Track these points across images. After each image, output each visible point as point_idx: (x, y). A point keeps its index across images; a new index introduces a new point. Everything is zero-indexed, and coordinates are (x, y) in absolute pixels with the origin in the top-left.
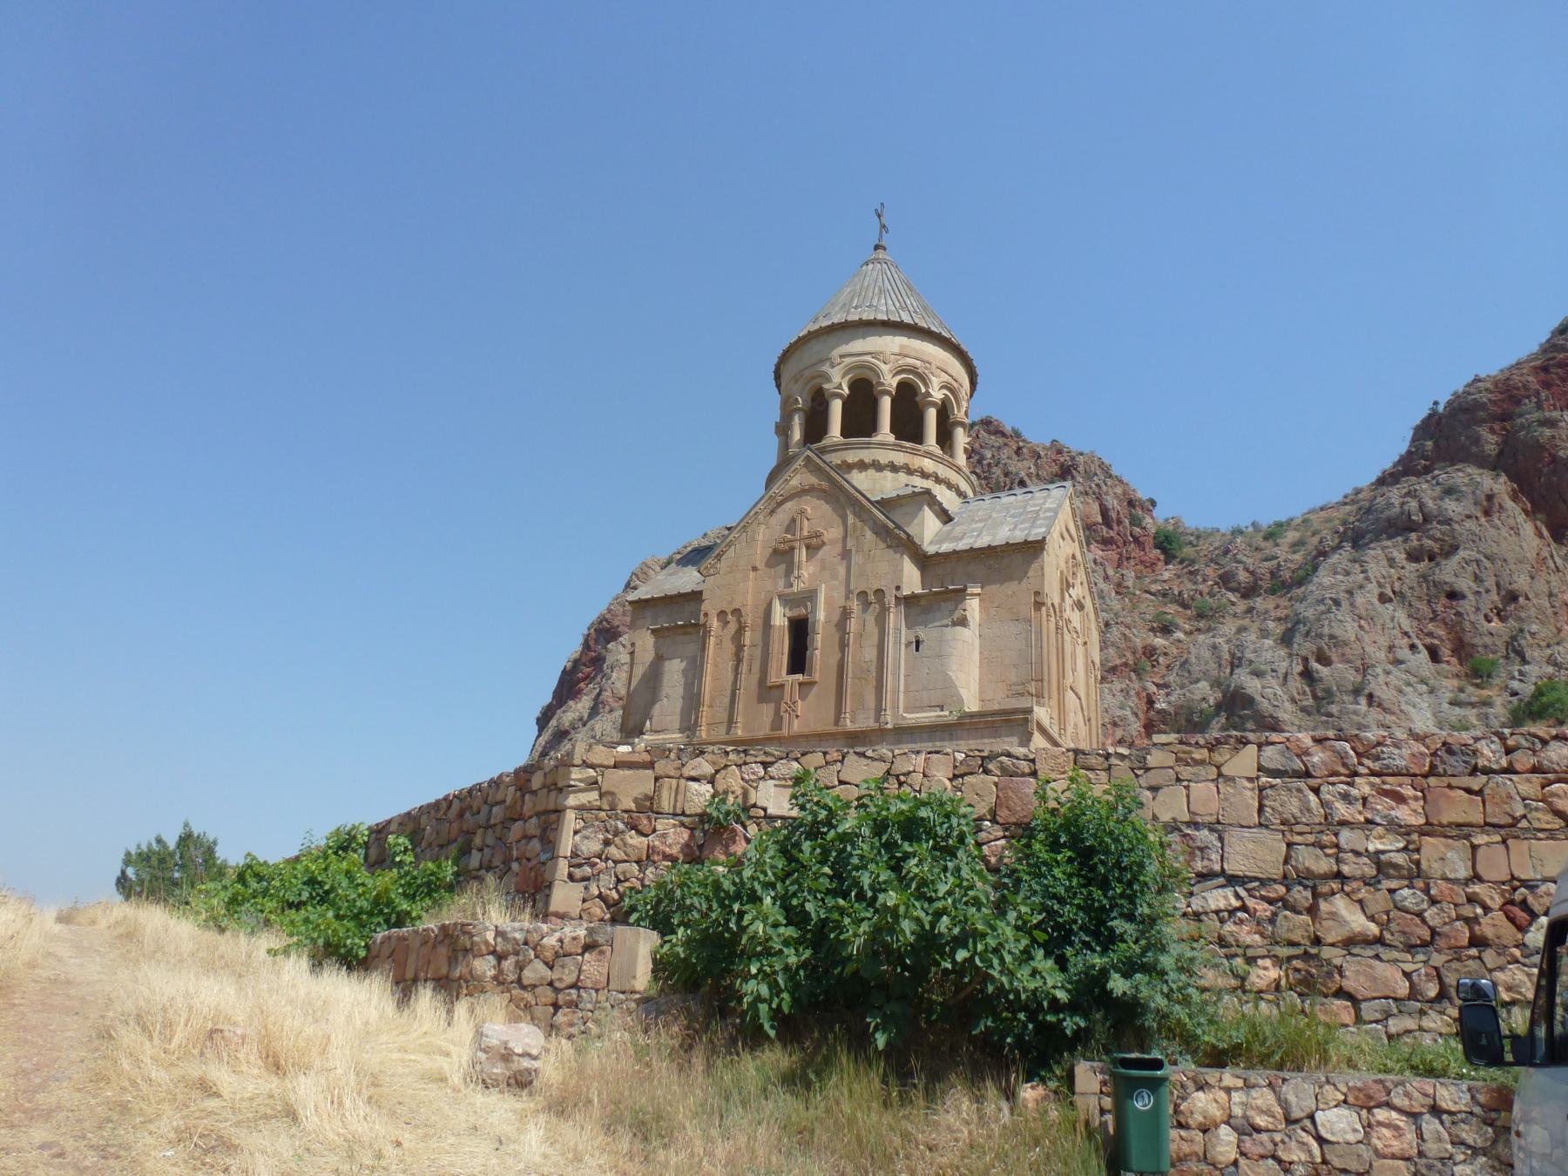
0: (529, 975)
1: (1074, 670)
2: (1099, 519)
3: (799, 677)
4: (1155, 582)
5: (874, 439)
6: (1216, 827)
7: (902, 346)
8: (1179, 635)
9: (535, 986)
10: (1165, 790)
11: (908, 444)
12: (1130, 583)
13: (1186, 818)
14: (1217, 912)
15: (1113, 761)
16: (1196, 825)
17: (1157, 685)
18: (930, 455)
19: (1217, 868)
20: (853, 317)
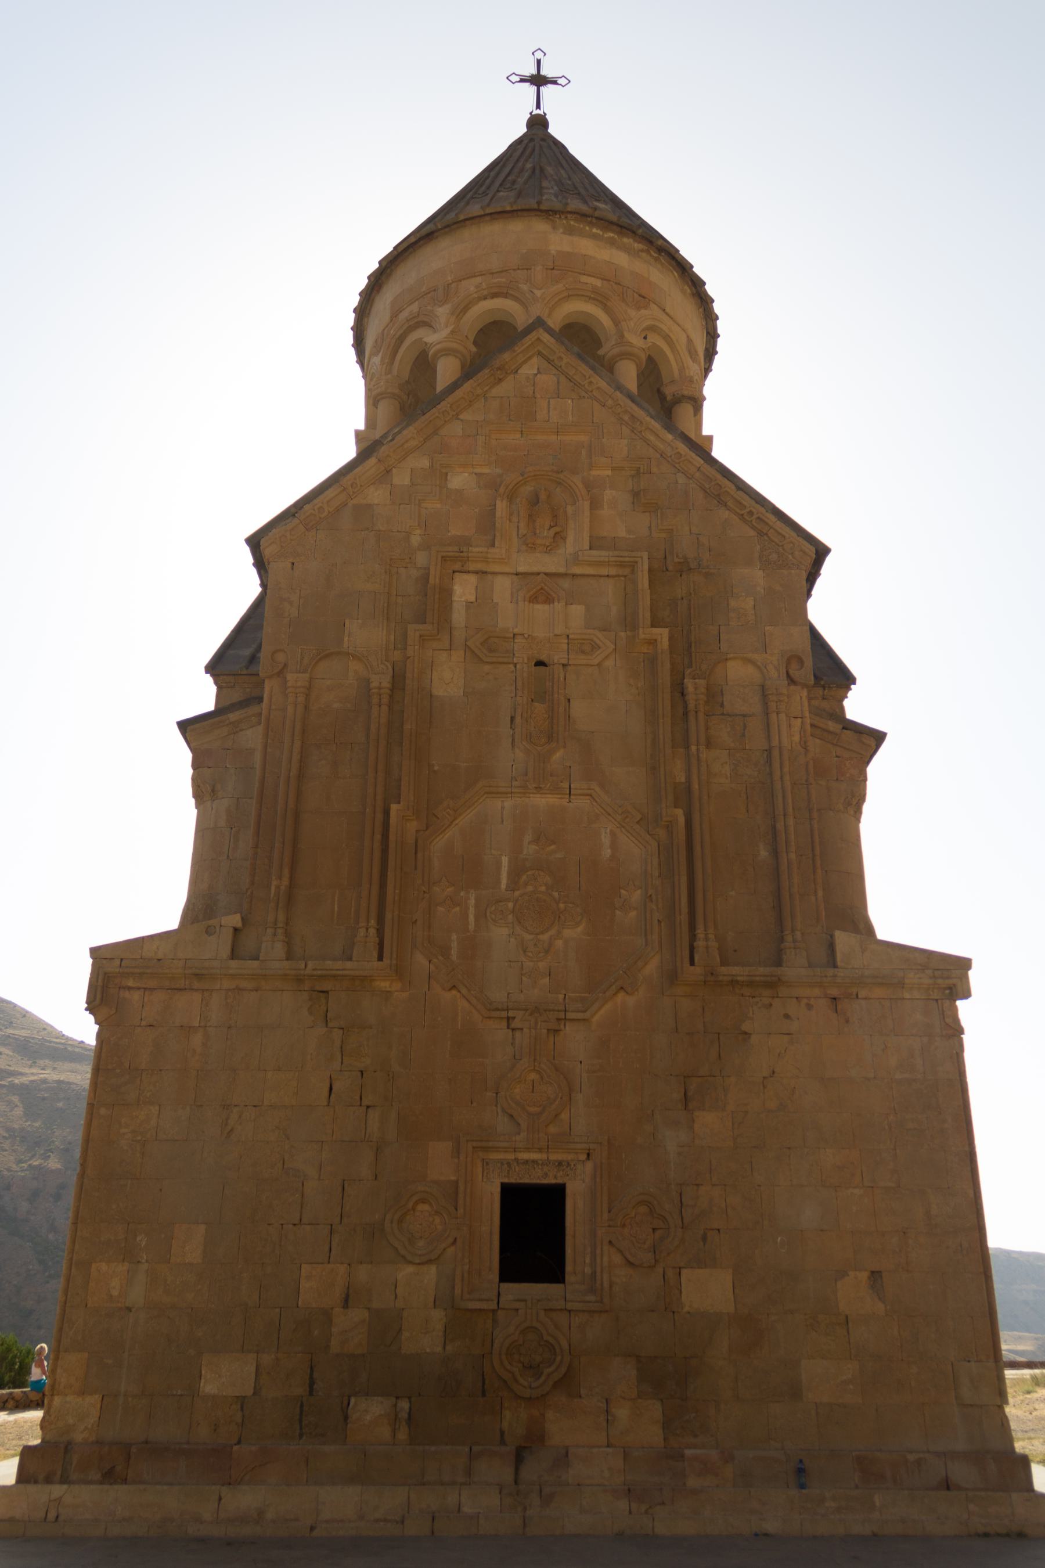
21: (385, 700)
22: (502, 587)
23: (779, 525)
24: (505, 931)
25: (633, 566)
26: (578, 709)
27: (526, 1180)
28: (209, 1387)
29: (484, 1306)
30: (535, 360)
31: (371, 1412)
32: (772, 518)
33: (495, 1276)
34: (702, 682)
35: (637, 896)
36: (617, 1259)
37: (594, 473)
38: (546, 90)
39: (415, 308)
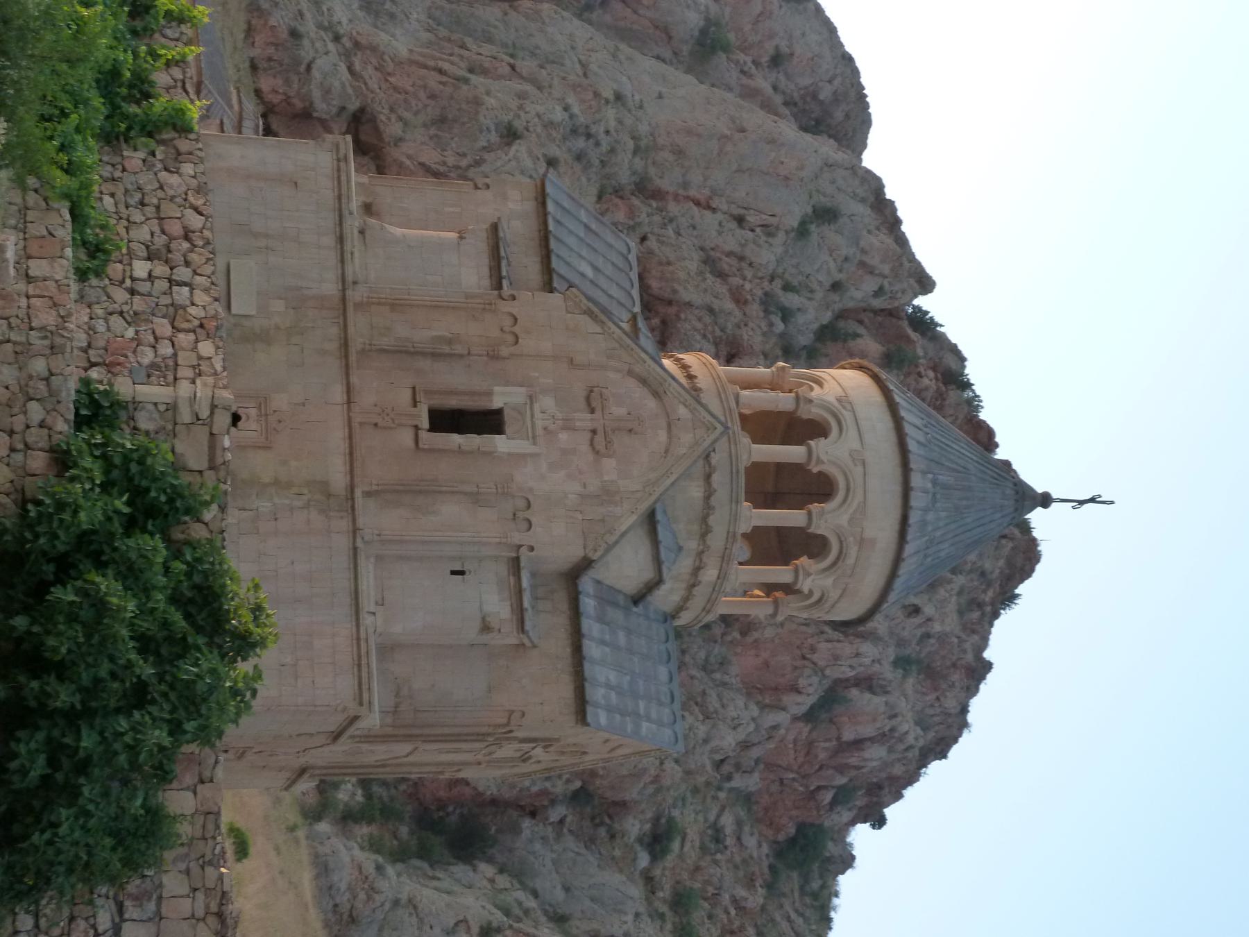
0: (33, 406)
1: (440, 752)
2: (848, 736)
3: (425, 423)
4: (739, 824)
6: (159, 916)
8: (644, 860)
9: (25, 413)
10: (186, 881)
12: (737, 782)
13: (164, 895)
14: (94, 916)
15: (210, 842)
16: (159, 904)
17: (562, 821)
18: (722, 576)
19: (126, 916)
20: (916, 480)
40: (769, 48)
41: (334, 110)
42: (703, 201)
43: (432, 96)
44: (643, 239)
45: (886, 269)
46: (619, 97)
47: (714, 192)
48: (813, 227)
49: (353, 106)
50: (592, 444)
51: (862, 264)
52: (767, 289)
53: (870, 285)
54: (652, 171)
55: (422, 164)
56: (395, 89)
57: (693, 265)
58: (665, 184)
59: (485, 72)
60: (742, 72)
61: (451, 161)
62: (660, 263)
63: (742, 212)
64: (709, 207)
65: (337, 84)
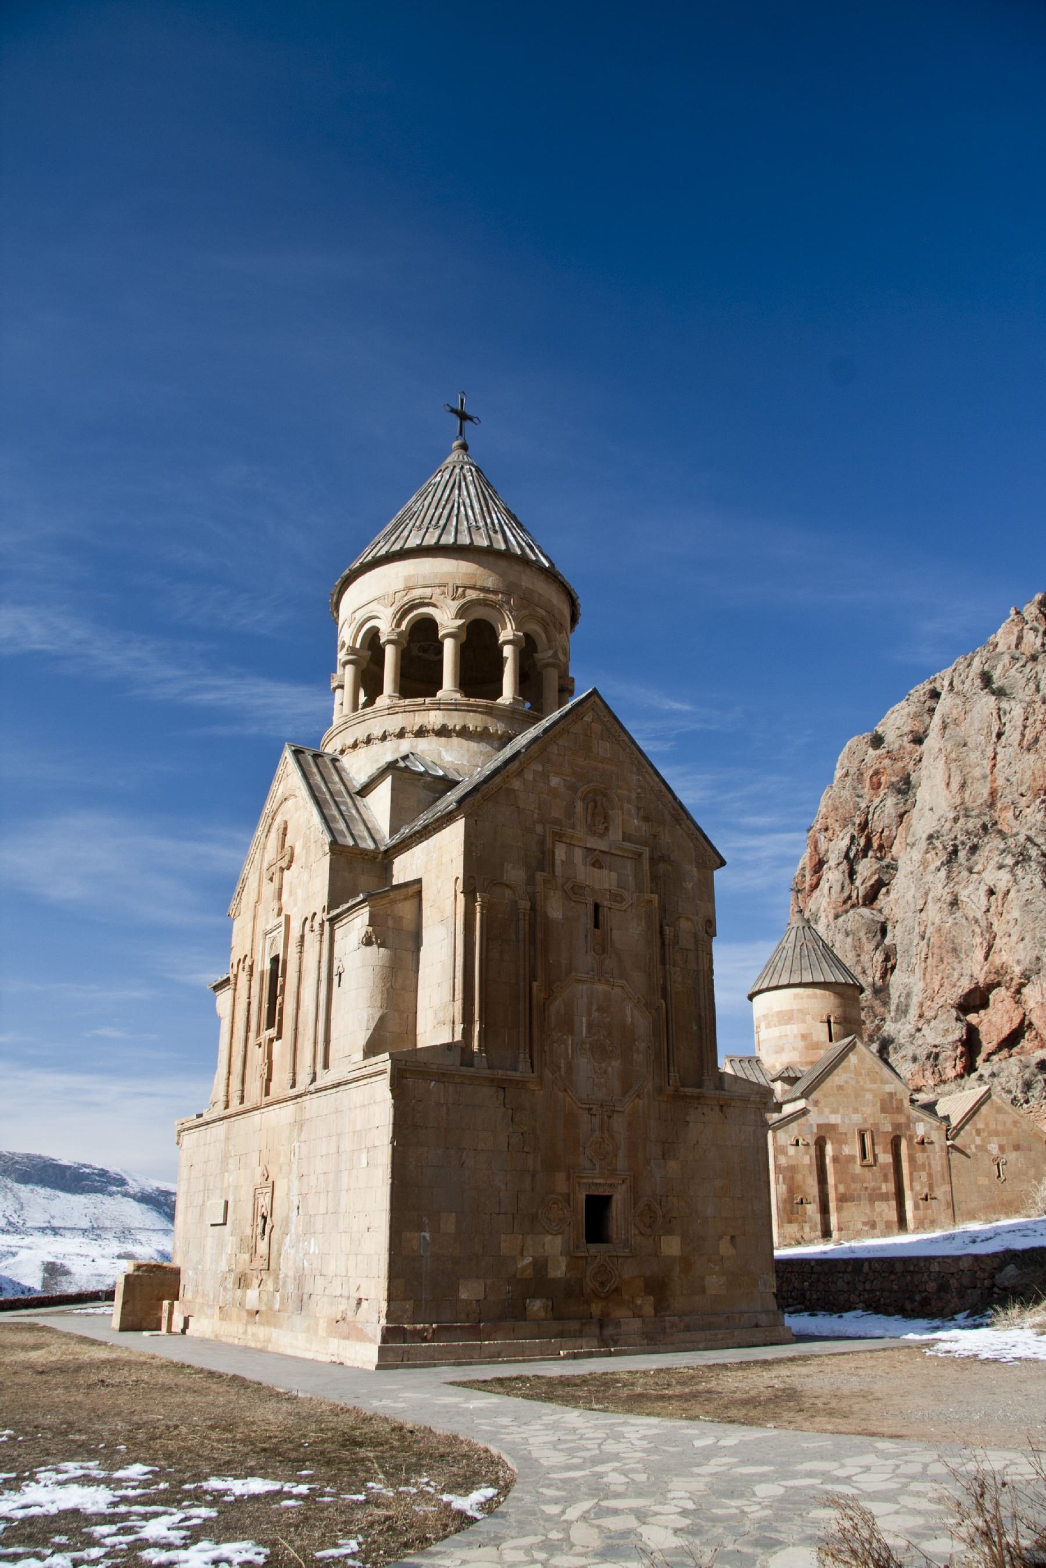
5: (375, 706)
7: (407, 579)
11: (407, 701)
18: (438, 706)
21: (527, 918)
22: (578, 853)
23: (705, 844)
24: (585, 1060)
25: (640, 855)
26: (616, 934)
27: (597, 1193)
28: (464, 1295)
29: (583, 1254)
30: (591, 714)
31: (536, 1306)
32: (702, 839)
33: (584, 1240)
34: (672, 929)
35: (642, 1046)
36: (637, 1232)
37: (620, 791)
38: (467, 424)
39: (428, 592)
40: (910, 747)
41: (959, 1024)
42: (992, 763)
43: (942, 960)
44: (1022, 795)
45: (1016, 630)
46: (930, 837)
47: (983, 757)
48: (994, 686)
49: (954, 1013)
50: (288, 868)
51: (1017, 646)
52: (1040, 703)
53: (1029, 636)
54: (979, 801)
55: (986, 958)
56: (942, 986)
57: (1032, 757)
58: (986, 792)
59: (924, 932)
60: (920, 760)
61: (978, 940)
62: (1035, 779)
63: (994, 735)
64: (994, 758)
65: (941, 1026)
